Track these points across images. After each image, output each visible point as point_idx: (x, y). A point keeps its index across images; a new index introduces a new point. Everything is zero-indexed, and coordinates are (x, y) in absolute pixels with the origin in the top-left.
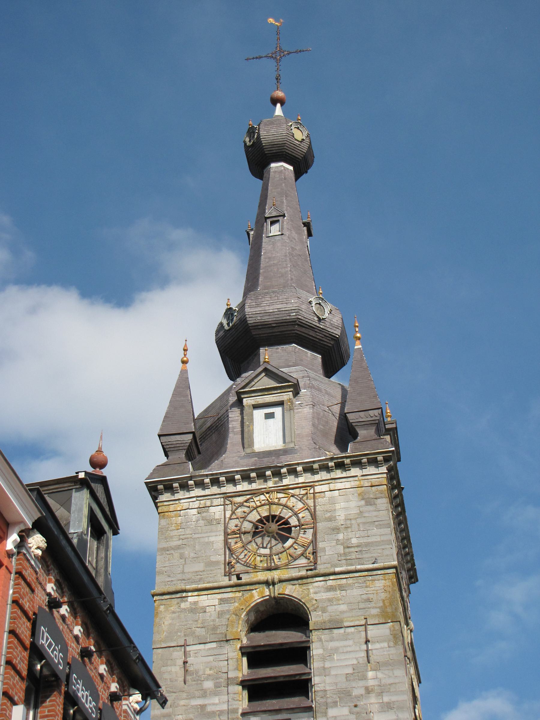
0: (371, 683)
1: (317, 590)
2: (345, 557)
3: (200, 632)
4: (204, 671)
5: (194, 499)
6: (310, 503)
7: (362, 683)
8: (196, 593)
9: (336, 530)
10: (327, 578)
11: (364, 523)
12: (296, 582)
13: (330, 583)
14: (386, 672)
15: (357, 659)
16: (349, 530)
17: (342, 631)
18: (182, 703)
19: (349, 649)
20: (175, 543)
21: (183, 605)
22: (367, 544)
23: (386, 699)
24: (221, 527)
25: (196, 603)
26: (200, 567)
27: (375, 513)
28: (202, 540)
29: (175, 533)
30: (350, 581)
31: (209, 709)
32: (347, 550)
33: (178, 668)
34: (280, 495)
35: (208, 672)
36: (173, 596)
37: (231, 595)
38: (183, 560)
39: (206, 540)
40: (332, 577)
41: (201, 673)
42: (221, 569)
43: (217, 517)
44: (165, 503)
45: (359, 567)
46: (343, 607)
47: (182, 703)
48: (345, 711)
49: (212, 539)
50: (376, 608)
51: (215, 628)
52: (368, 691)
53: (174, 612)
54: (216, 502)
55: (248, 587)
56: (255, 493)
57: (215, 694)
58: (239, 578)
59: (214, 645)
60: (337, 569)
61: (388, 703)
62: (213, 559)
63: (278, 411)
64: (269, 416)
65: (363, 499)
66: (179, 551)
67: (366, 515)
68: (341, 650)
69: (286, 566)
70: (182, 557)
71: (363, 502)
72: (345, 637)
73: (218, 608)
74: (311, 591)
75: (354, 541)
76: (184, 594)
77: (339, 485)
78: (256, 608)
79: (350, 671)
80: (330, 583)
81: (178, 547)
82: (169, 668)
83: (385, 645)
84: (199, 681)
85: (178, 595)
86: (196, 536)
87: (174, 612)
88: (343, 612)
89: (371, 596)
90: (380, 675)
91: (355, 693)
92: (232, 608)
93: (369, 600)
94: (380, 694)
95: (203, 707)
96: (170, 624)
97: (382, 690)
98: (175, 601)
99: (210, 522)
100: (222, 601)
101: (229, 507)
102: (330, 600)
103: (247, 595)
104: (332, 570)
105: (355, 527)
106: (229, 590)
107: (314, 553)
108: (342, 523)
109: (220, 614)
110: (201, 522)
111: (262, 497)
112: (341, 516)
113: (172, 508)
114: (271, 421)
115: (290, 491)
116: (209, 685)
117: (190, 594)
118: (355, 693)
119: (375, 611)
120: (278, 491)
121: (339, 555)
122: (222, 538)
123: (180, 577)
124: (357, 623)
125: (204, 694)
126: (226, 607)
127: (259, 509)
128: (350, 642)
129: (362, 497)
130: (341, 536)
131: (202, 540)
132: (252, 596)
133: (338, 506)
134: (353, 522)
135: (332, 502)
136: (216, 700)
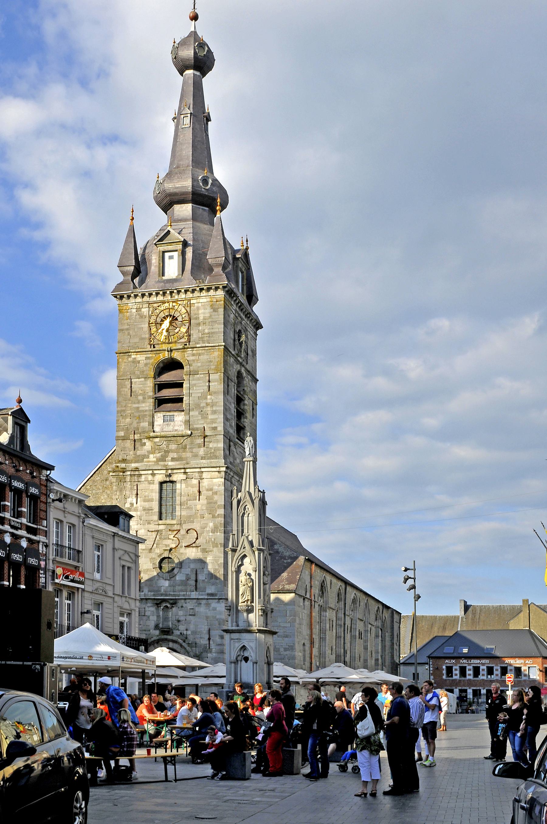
0: (209, 401)
1: (188, 355)
2: (202, 339)
3: (137, 373)
4: (139, 391)
5: (135, 304)
6: (188, 309)
7: (204, 401)
8: (135, 353)
9: (199, 324)
10: (193, 349)
11: (212, 322)
12: (179, 350)
13: (194, 352)
14: (216, 396)
15: (204, 389)
16: (205, 325)
17: (198, 376)
18: (129, 405)
19: (200, 385)
20: (126, 327)
21: (129, 359)
22: (213, 333)
23: (214, 409)
24: (147, 319)
25: (135, 358)
26: (137, 340)
27: (217, 316)
28: (138, 326)
29: (126, 321)
30: (203, 351)
31: (140, 409)
32: (203, 336)
33: (127, 389)
34: (174, 304)
35: (140, 392)
36: (125, 354)
37: (150, 355)
38: (129, 336)
39: (140, 326)
40: (195, 349)
41: (137, 392)
42: (147, 342)
43: (145, 314)
44: (121, 305)
45: (207, 345)
46: (199, 364)
47: (129, 405)
48: (197, 413)
49: (143, 326)
50: (214, 365)
51: (143, 372)
52: (207, 404)
53: (125, 362)
54: (145, 306)
55: (158, 352)
56: (164, 302)
57: (143, 402)
58: (154, 347)
59: (143, 379)
60: (198, 346)
61: (215, 411)
62: (143, 336)
63: (175, 254)
64: (171, 257)
65: (212, 308)
66: (128, 331)
67: (213, 317)
68: (197, 385)
69: (175, 342)
70: (129, 334)
71: (212, 310)
72: (199, 379)
73: (145, 362)
74: (186, 355)
75: (206, 331)
76: (130, 354)
77: (201, 301)
78: (163, 362)
79: (200, 395)
80: (194, 352)
81: (127, 329)
82: (124, 389)
83: (216, 383)
84: (137, 396)
85: (127, 354)
86: (135, 324)
87: (125, 362)
88: (199, 367)
89: (212, 359)
90: (213, 398)
91: (202, 405)
92: (151, 362)
93: (211, 361)
94: (212, 406)
95: (138, 408)
96: (124, 368)
97: (213, 404)
98: (126, 357)
99: (142, 316)
100: (147, 358)
101: (151, 309)
102: (194, 361)
103: (157, 356)
104: (195, 346)
105: (207, 323)
106: (150, 353)
107: (189, 336)
108: (202, 321)
109: (146, 365)
110: (138, 316)
111: (167, 304)
112: (201, 317)
113: (124, 308)
114: (171, 260)
115: (179, 302)
116: (140, 398)
117: (132, 354)
118: (202, 405)
119: (213, 367)
120: (173, 302)
121: (200, 338)
122: (147, 325)
123: (128, 345)
124: (205, 372)
125: (138, 403)
126: (148, 361)
127: (164, 311)
128: (201, 382)
129: (212, 306)
130: (201, 328)
131: (138, 326)
132: (160, 357)
133: (200, 312)
134: (207, 320)
135: (198, 308)
136: (143, 405)
